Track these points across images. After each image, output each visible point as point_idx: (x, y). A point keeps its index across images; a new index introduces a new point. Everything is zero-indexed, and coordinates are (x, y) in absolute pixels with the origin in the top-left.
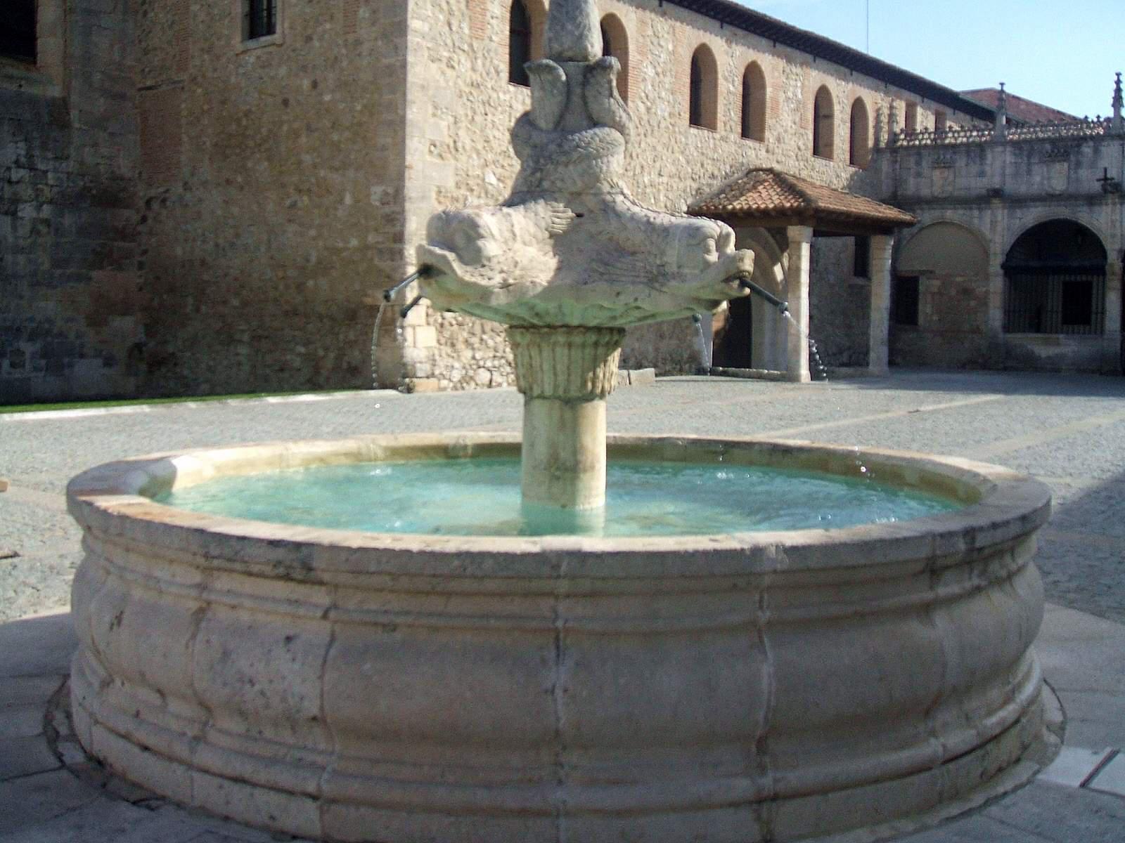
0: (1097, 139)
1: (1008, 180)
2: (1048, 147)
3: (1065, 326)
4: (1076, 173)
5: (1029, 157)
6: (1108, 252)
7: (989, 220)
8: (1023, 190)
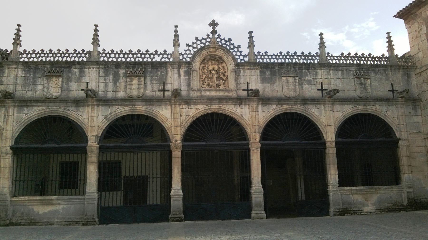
0: (82, 65)
1: (19, 88)
2: (48, 67)
3: (61, 190)
4: (68, 84)
5: (35, 73)
6: (89, 138)
7: (3, 115)
8: (29, 94)
